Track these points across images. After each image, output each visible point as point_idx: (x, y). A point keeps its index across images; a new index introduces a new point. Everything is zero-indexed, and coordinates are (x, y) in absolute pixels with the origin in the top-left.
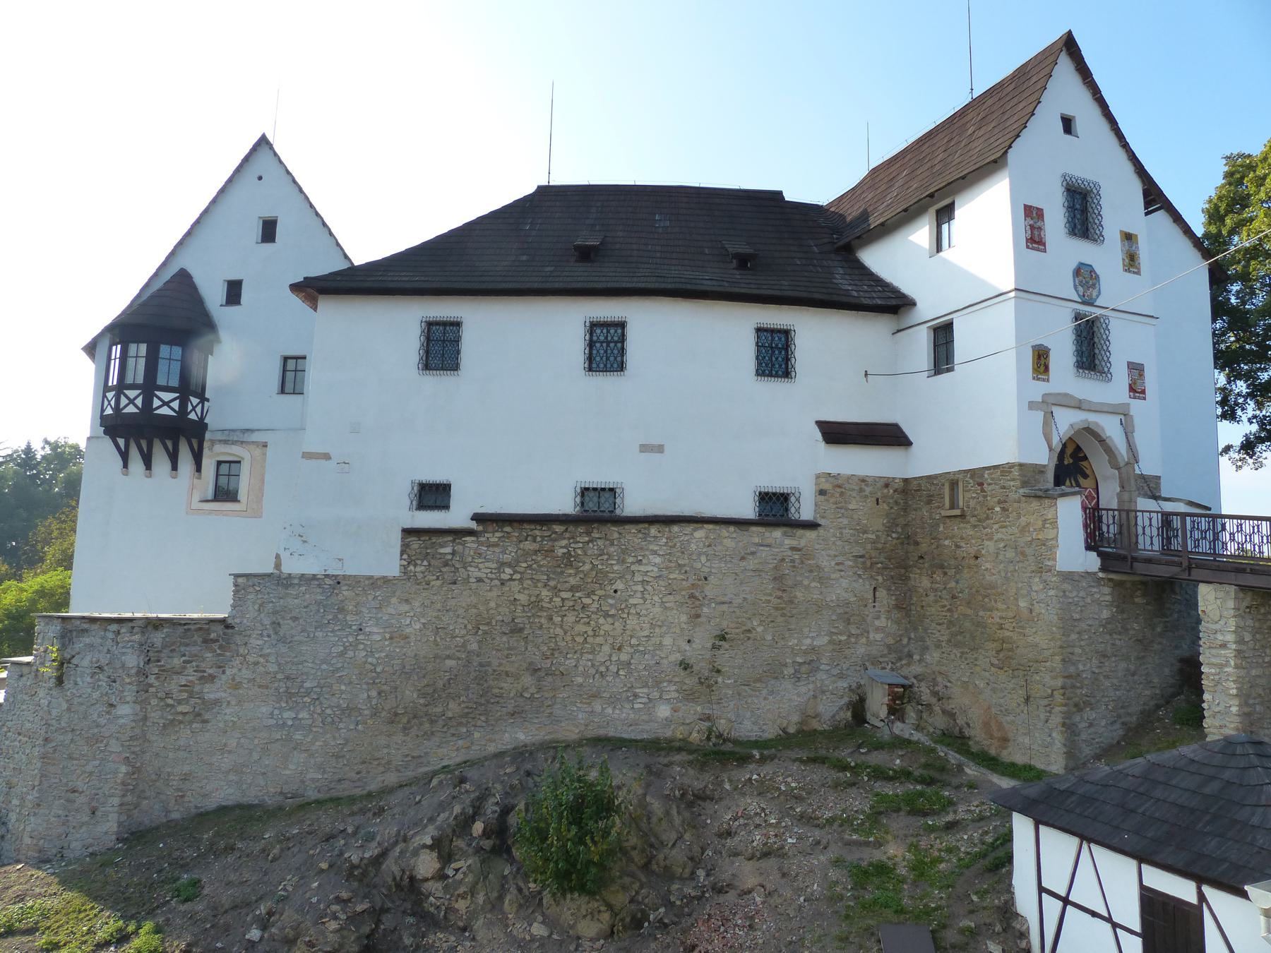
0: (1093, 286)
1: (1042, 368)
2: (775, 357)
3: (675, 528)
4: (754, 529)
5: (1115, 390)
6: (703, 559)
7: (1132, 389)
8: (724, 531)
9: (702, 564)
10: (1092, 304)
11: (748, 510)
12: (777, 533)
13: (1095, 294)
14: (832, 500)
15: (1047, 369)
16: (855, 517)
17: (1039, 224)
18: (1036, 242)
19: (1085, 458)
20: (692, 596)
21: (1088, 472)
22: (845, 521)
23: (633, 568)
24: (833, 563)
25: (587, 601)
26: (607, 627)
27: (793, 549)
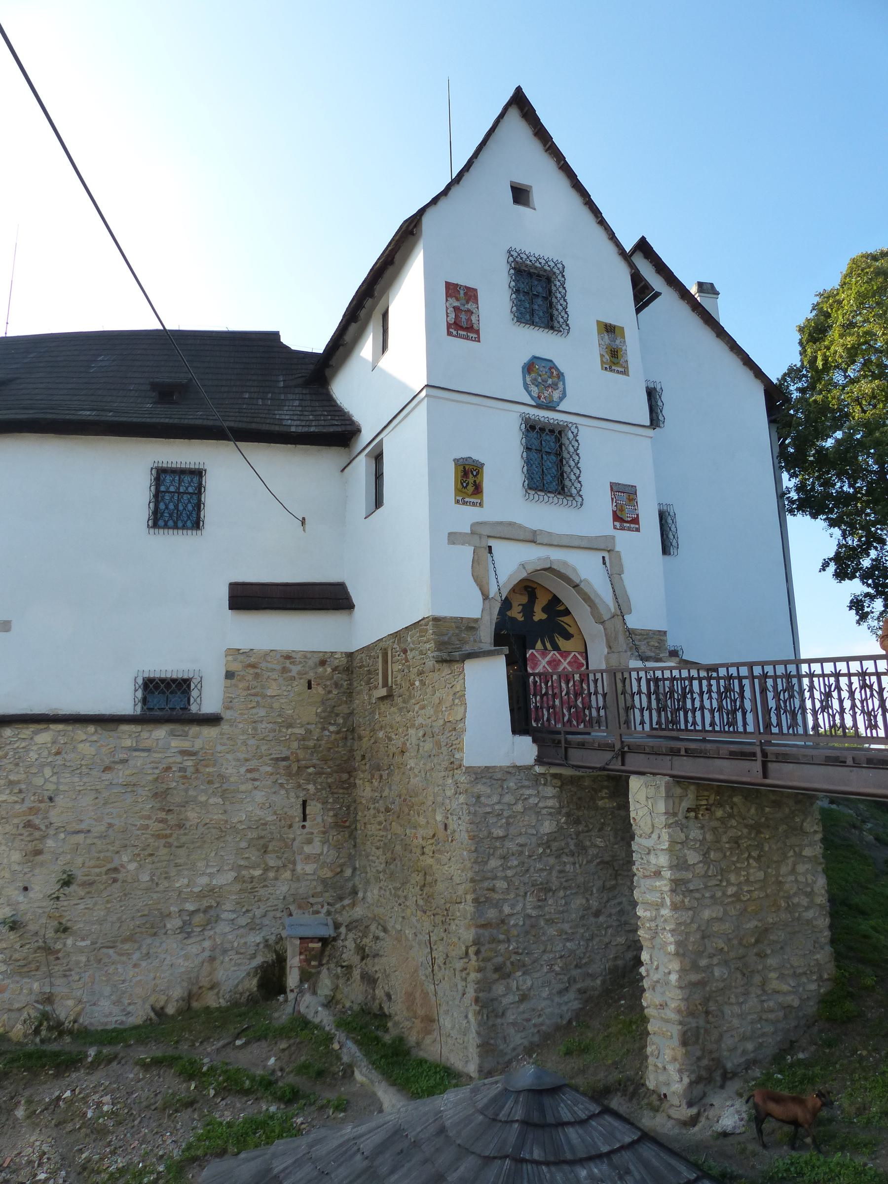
0: (554, 386)
1: (471, 488)
4: (125, 728)
5: (593, 515)
6: (48, 772)
7: (616, 517)
8: (80, 733)
10: (553, 409)
11: (125, 701)
12: (160, 733)
13: (556, 395)
14: (241, 685)
15: (478, 490)
16: (276, 705)
17: (469, 306)
18: (462, 328)
19: (567, 612)
20: (28, 825)
21: (571, 630)
22: (262, 712)
24: (243, 770)
27: (183, 753)
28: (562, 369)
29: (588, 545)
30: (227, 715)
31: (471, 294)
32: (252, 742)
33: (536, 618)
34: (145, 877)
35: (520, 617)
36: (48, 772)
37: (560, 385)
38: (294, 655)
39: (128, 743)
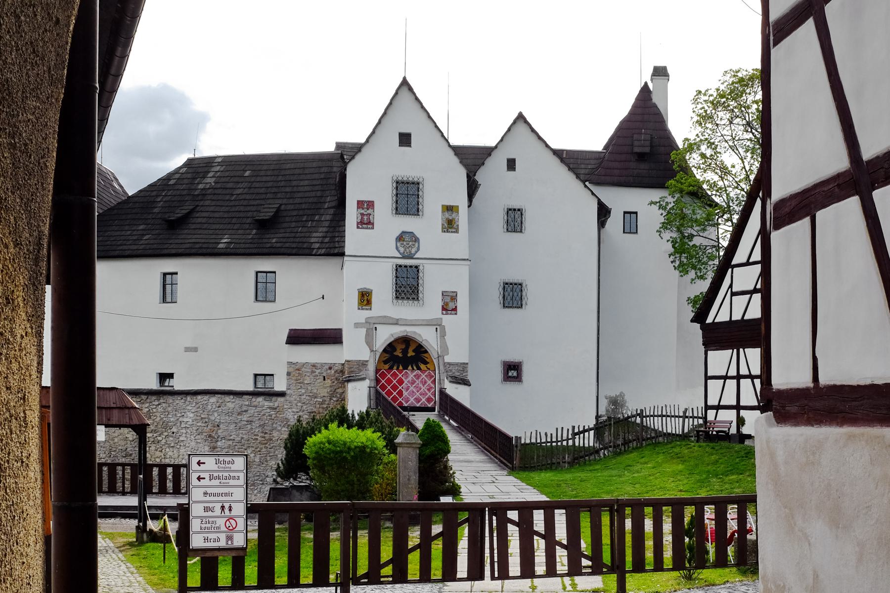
1: (365, 302)
2: (264, 290)
3: (199, 397)
6: (216, 414)
7: (444, 309)
8: (227, 398)
9: (215, 417)
10: (412, 258)
13: (413, 251)
15: (369, 302)
16: (309, 388)
17: (370, 211)
20: (210, 436)
23: (181, 419)
25: (160, 438)
26: (170, 453)
27: (270, 408)
29: (428, 323)
30: (288, 392)
31: (371, 204)
32: (299, 404)
34: (257, 460)
35: (400, 355)
36: (216, 414)
37: (417, 245)
39: (247, 403)
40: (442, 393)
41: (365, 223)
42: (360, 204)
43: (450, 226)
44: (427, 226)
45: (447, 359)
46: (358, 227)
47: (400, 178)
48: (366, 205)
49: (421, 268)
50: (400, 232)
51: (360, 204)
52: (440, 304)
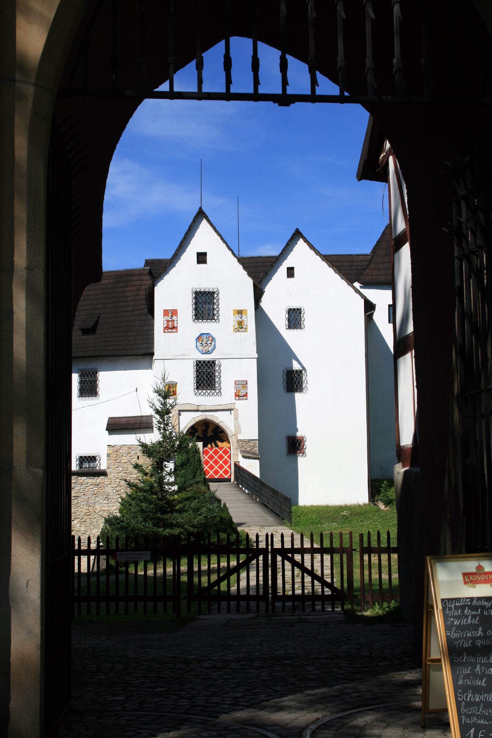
7: (237, 395)
17: (174, 318)
24: (115, 491)
28: (214, 336)
30: (108, 471)
31: (174, 312)
32: (118, 480)
33: (209, 435)
37: (213, 344)
38: (132, 447)
40: (238, 468)
41: (171, 328)
42: (166, 312)
43: (241, 326)
44: (221, 329)
45: (240, 437)
46: (165, 332)
47: (198, 290)
48: (171, 313)
49: (217, 362)
50: (199, 334)
51: (166, 312)
52: (234, 391)
